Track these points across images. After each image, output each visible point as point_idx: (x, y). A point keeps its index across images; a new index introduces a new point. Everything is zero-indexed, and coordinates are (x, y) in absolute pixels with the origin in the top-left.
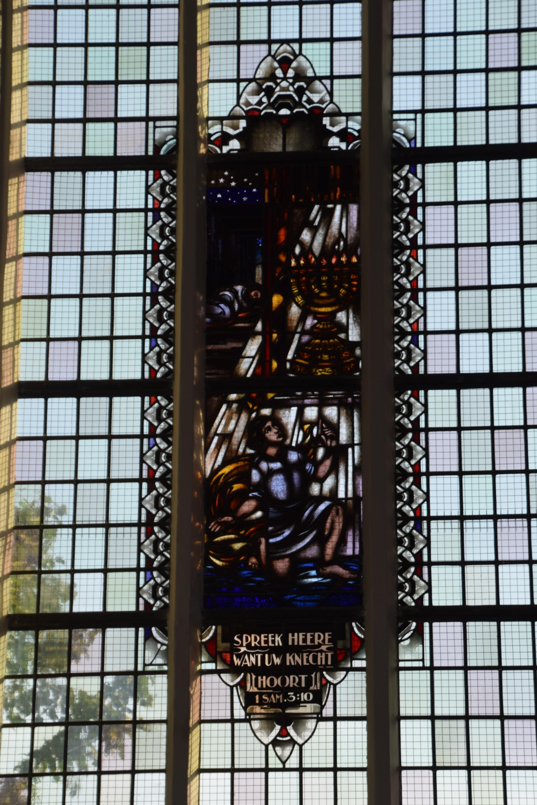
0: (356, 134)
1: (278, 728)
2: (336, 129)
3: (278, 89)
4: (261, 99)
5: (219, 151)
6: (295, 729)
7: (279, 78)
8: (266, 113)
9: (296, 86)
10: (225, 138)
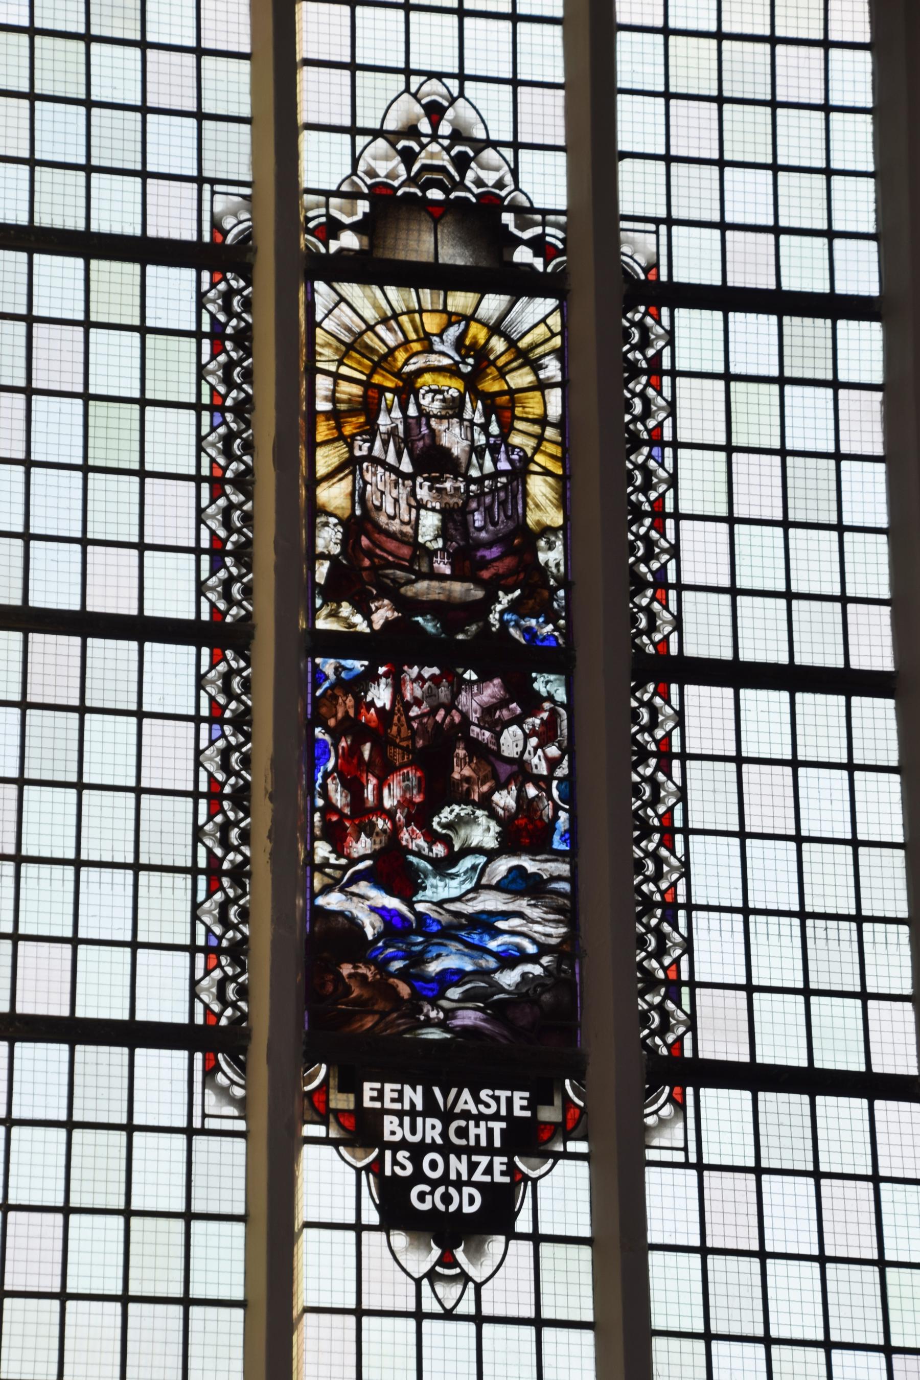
0: (561, 246)
1: (436, 1252)
2: (527, 235)
3: (423, 154)
4: (395, 168)
7: (426, 136)
8: (405, 194)
9: (453, 153)
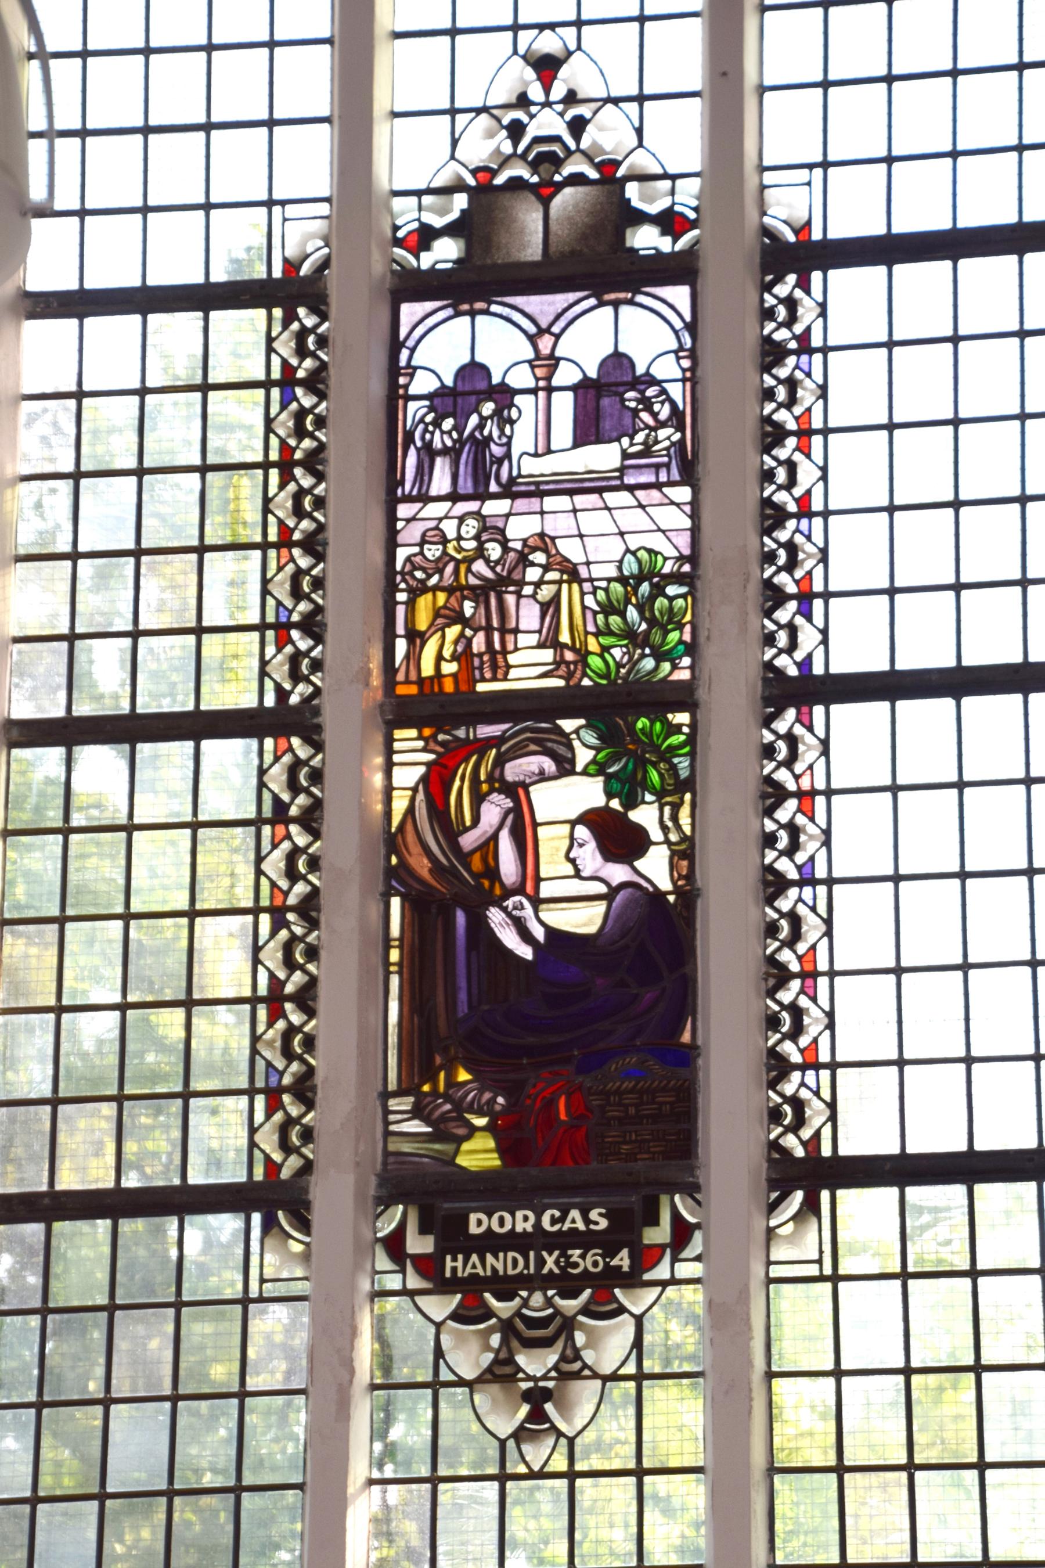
1: (525, 1409)
5: (415, 263)
10: (426, 236)
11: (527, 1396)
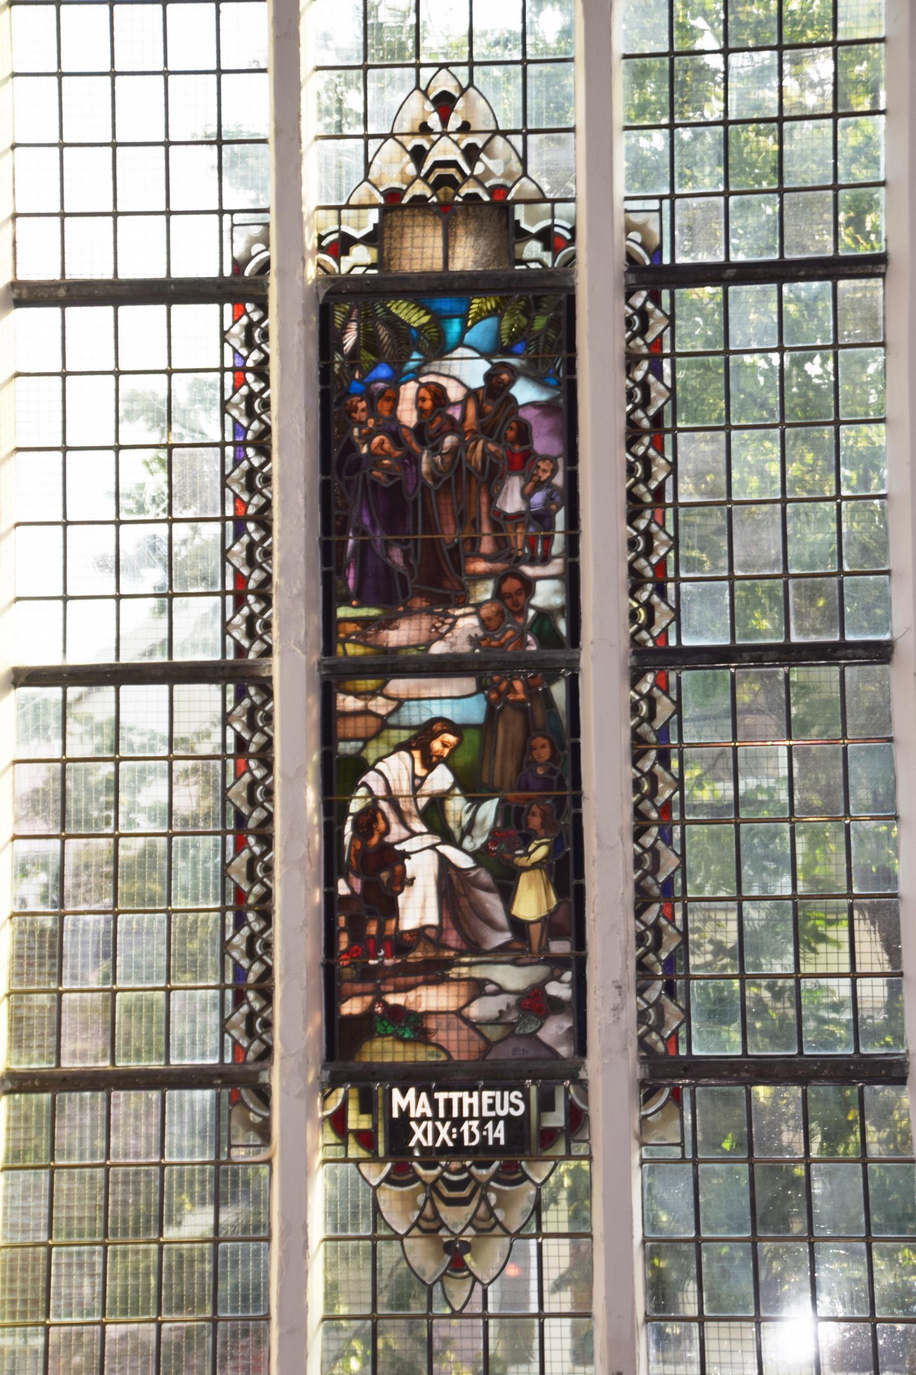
1: (448, 1258)
2: (534, 230)
6: (474, 1258)
11: (448, 1248)
